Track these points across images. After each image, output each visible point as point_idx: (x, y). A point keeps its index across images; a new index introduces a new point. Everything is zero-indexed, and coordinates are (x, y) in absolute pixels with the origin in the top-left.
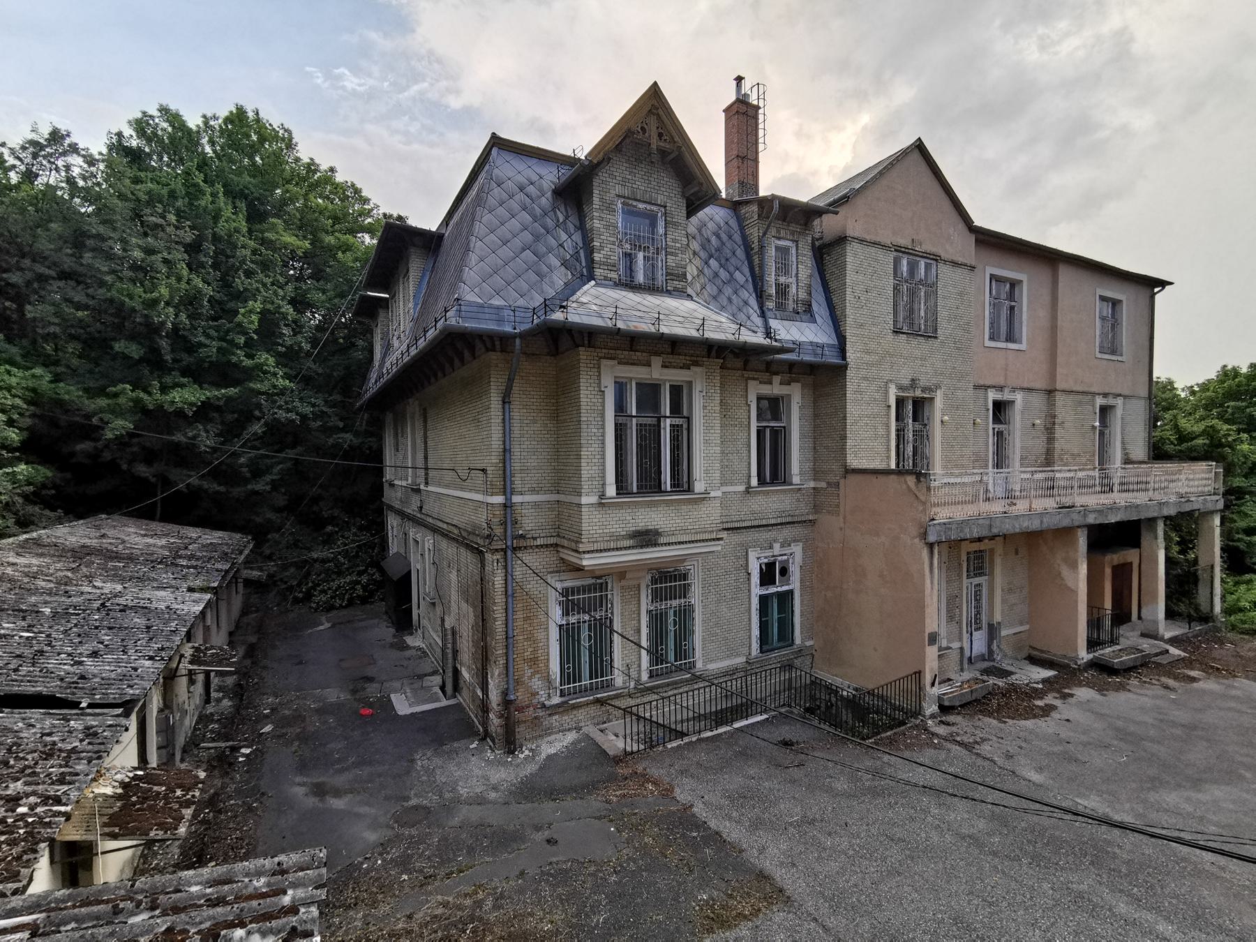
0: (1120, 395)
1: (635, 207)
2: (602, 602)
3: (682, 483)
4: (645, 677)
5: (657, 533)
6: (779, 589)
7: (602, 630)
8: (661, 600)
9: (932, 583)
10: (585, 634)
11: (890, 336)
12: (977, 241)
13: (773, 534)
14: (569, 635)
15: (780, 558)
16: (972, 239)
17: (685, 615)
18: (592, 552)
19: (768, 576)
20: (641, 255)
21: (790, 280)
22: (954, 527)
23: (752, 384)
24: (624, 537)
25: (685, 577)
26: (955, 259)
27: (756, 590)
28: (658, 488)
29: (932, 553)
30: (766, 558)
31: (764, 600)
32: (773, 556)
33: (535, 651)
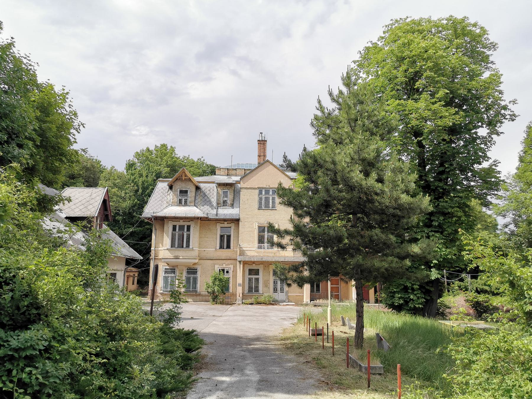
3: (188, 246)
9: (240, 271)
11: (257, 210)
13: (224, 261)
14: (166, 278)
17: (195, 280)
28: (183, 247)
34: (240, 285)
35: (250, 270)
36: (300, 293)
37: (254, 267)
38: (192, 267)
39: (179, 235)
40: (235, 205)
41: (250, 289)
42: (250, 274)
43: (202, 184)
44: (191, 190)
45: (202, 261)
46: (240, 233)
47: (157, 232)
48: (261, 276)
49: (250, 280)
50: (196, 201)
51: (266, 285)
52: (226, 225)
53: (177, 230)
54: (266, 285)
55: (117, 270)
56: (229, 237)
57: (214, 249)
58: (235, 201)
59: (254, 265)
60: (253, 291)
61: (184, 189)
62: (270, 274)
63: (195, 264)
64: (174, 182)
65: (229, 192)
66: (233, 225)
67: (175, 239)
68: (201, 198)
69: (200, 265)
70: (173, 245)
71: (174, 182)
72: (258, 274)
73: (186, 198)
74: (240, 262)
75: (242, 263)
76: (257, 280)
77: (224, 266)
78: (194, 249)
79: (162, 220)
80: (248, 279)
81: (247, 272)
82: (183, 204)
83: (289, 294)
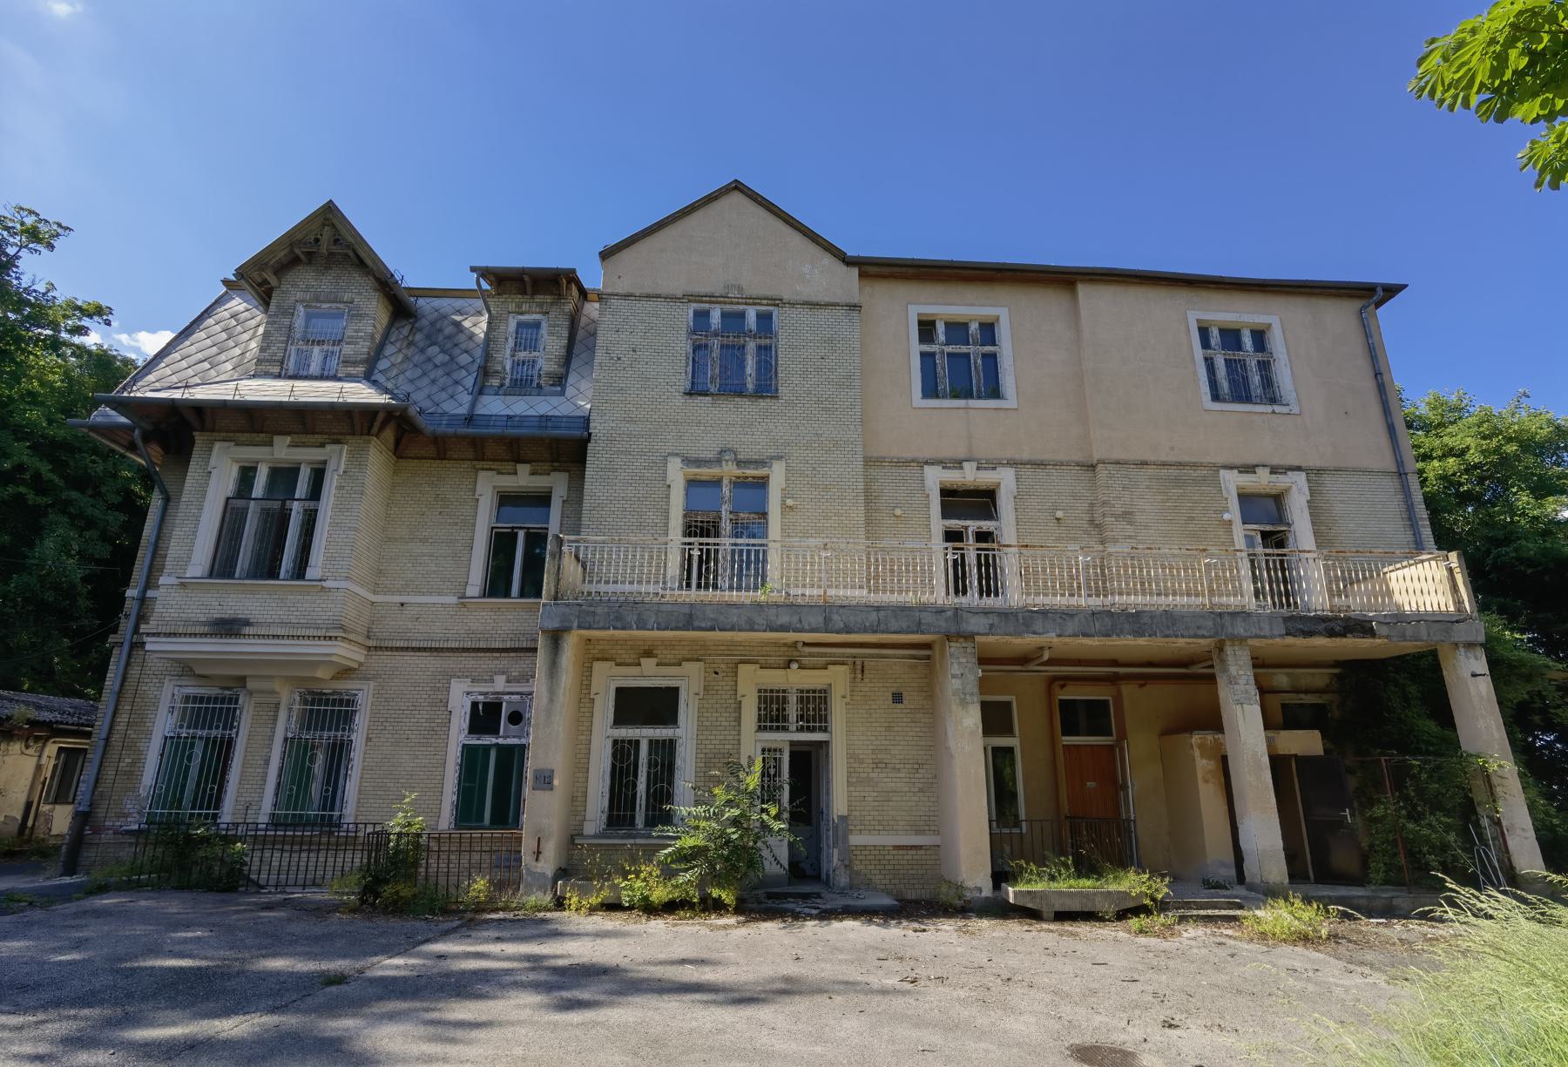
0: (1299, 469)
1: (319, 308)
3: (300, 571)
4: (263, 819)
5: (247, 623)
6: (501, 741)
7: (222, 751)
8: (316, 729)
9: (552, 692)
10: (198, 751)
11: (679, 401)
12: (860, 275)
13: (504, 662)
15: (506, 697)
16: (854, 272)
17: (339, 754)
18: (158, 634)
19: (485, 717)
21: (536, 354)
22: (599, 610)
23: (483, 477)
24: (204, 624)
25: (349, 703)
26: (814, 299)
27: (458, 734)
28: (273, 573)
30: (481, 694)
31: (468, 750)
32: (497, 693)
36: (919, 832)
37: (649, 675)
38: (327, 688)
39: (266, 513)
40: (571, 379)
41: (620, 813)
42: (619, 721)
45: (385, 660)
46: (586, 505)
48: (686, 732)
49: (623, 754)
50: (383, 364)
52: (523, 479)
53: (258, 490)
56: (537, 540)
57: (453, 600)
58: (574, 365)
59: (648, 664)
62: (738, 720)
63: (346, 672)
65: (544, 325)
66: (558, 484)
69: (374, 678)
70: (222, 567)
76: (665, 753)
77: (500, 684)
80: (609, 750)
81: (605, 708)
83: (855, 840)
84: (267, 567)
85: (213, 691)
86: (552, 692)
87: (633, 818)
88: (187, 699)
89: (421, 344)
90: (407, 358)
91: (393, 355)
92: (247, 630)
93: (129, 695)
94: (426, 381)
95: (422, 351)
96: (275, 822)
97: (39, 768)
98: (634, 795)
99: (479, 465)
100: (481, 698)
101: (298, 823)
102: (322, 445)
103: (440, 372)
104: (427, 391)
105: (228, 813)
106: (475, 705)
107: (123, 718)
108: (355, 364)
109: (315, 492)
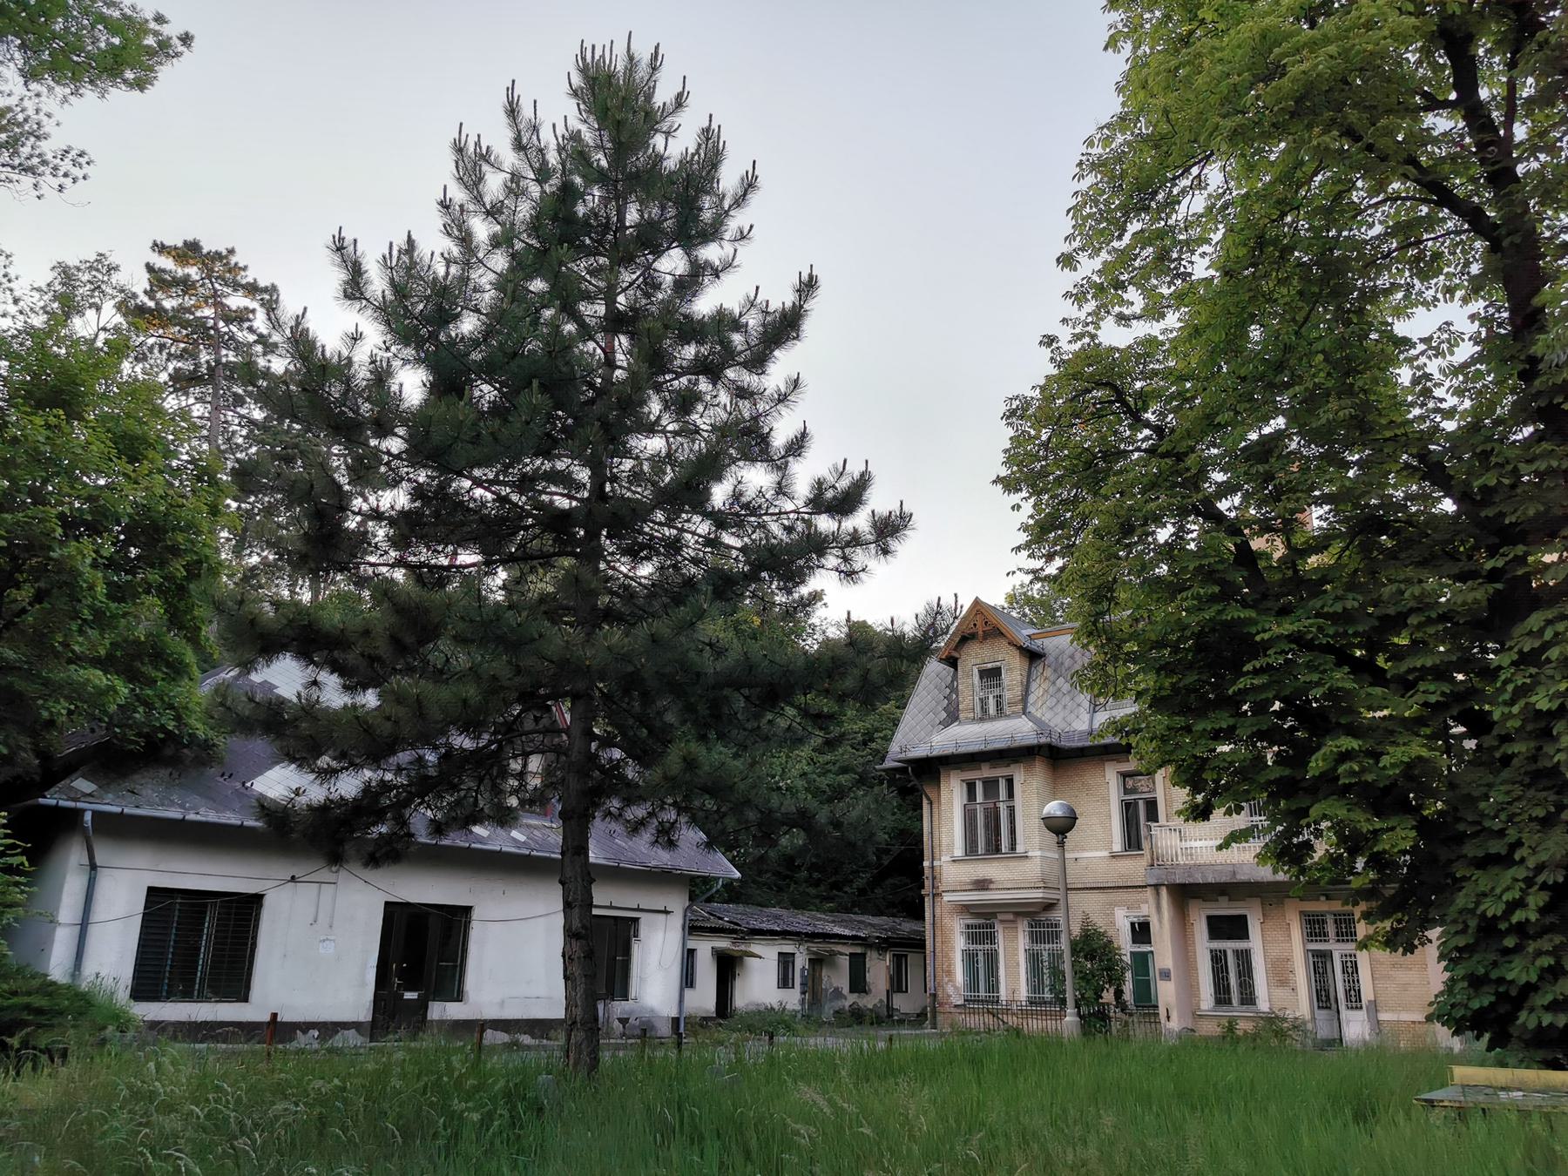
2: (991, 938)
3: (1013, 847)
5: (991, 882)
9: (1160, 921)
14: (970, 958)
20: (991, 697)
29: (1158, 894)
33: (949, 966)
34: (1166, 975)
35: (1210, 919)
37: (1224, 909)
43: (1051, 639)
44: (1009, 664)
47: (935, 810)
48: (1255, 942)
49: (1218, 959)
50: (1032, 699)
51: (1281, 976)
53: (980, 798)
54: (1281, 976)
55: (638, 910)
59: (1223, 900)
60: (1235, 1001)
61: (990, 666)
62: (1289, 936)
63: (1049, 906)
64: (956, 648)
67: (987, 826)
68: (1045, 686)
71: (956, 648)
72: (1244, 935)
73: (997, 692)
74: (1156, 887)
75: (1164, 892)
76: (1244, 958)
78: (1030, 854)
79: (930, 769)
81: (1200, 929)
82: (992, 710)
83: (1383, 1016)
84: (994, 848)
85: (982, 921)
86: (1160, 921)
87: (1230, 999)
88: (968, 927)
89: (1052, 678)
90: (1046, 691)
91: (1037, 691)
92: (992, 886)
93: (938, 925)
94: (1060, 707)
95: (1054, 683)
96: (1031, 1002)
97: (888, 968)
98: (1229, 985)
99: (1105, 757)
100: (1135, 920)
101: (1044, 1002)
102: (1008, 765)
103: (1068, 698)
104: (1062, 715)
105: (1003, 994)
106: (1133, 924)
107: (938, 939)
108: (1015, 704)
109: (1011, 795)
